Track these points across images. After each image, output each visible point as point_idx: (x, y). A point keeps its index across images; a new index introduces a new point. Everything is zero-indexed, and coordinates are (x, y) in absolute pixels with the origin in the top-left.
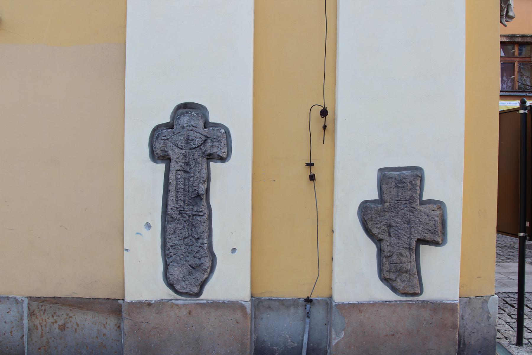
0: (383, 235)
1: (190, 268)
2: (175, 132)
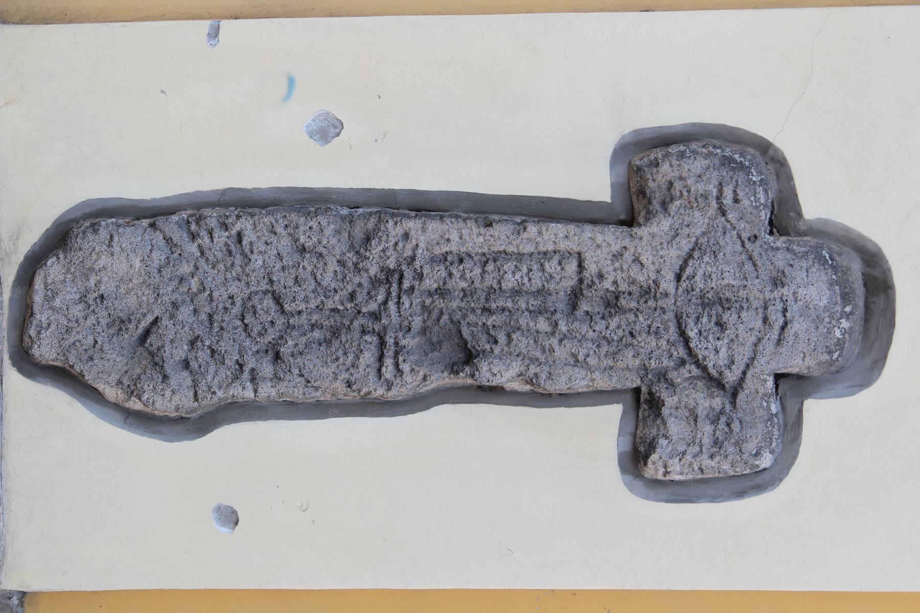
1: (144, 324)
2: (758, 243)
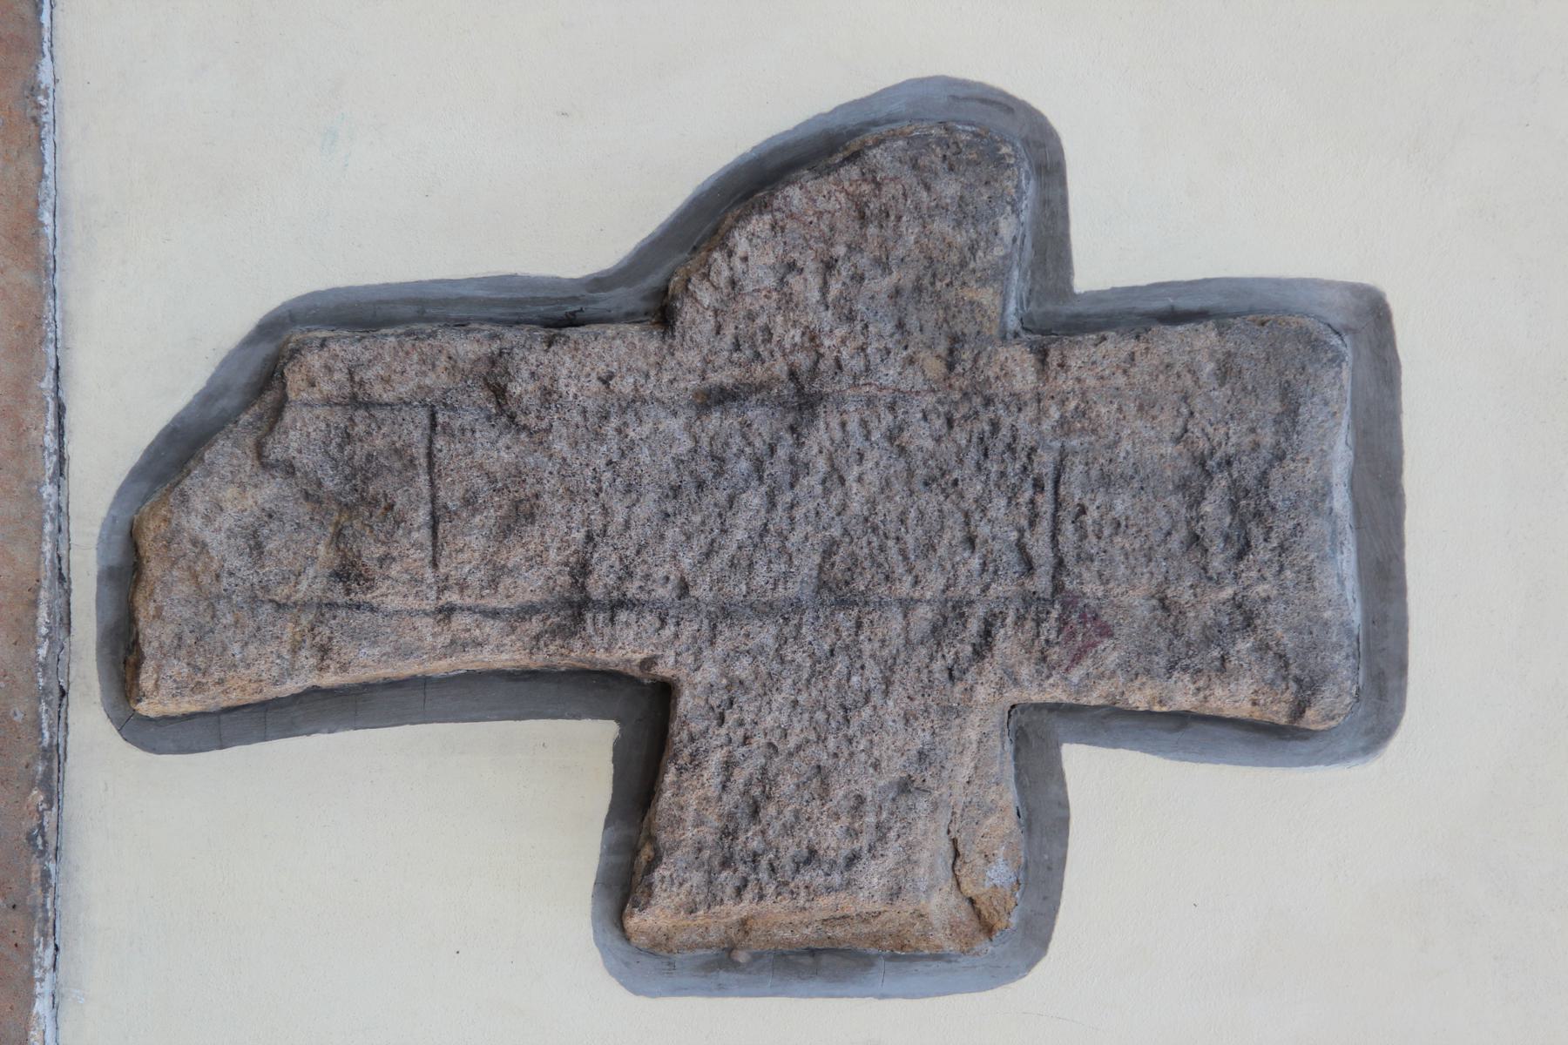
0: (718, 330)
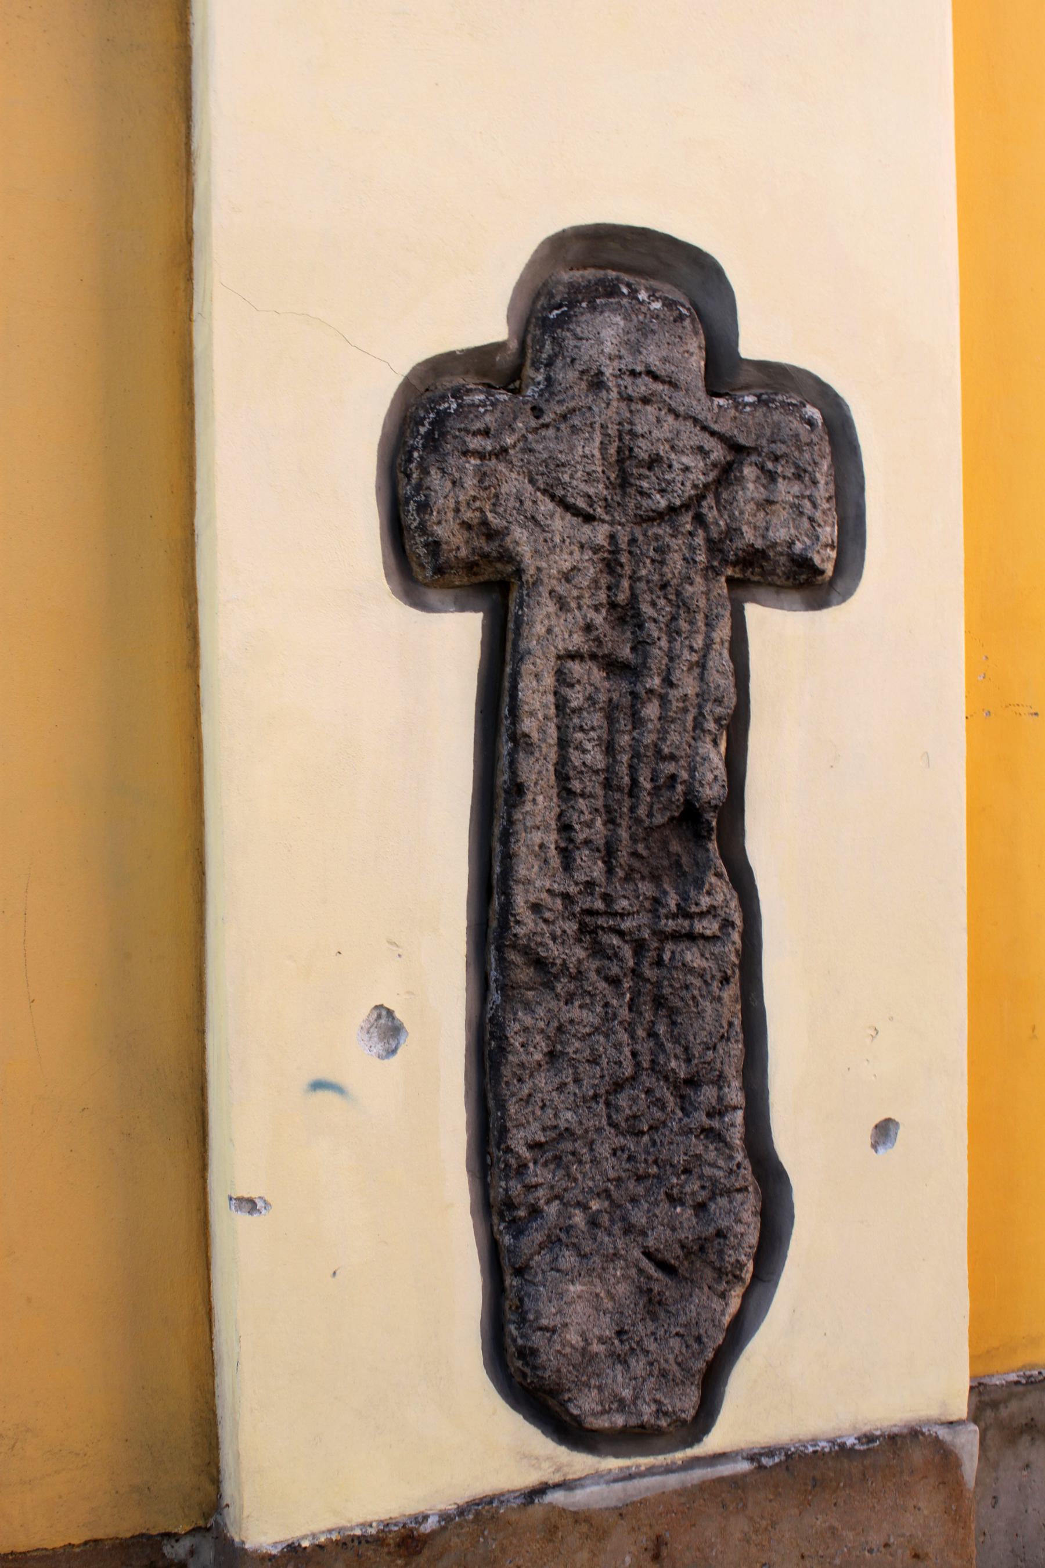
2: (543, 405)
